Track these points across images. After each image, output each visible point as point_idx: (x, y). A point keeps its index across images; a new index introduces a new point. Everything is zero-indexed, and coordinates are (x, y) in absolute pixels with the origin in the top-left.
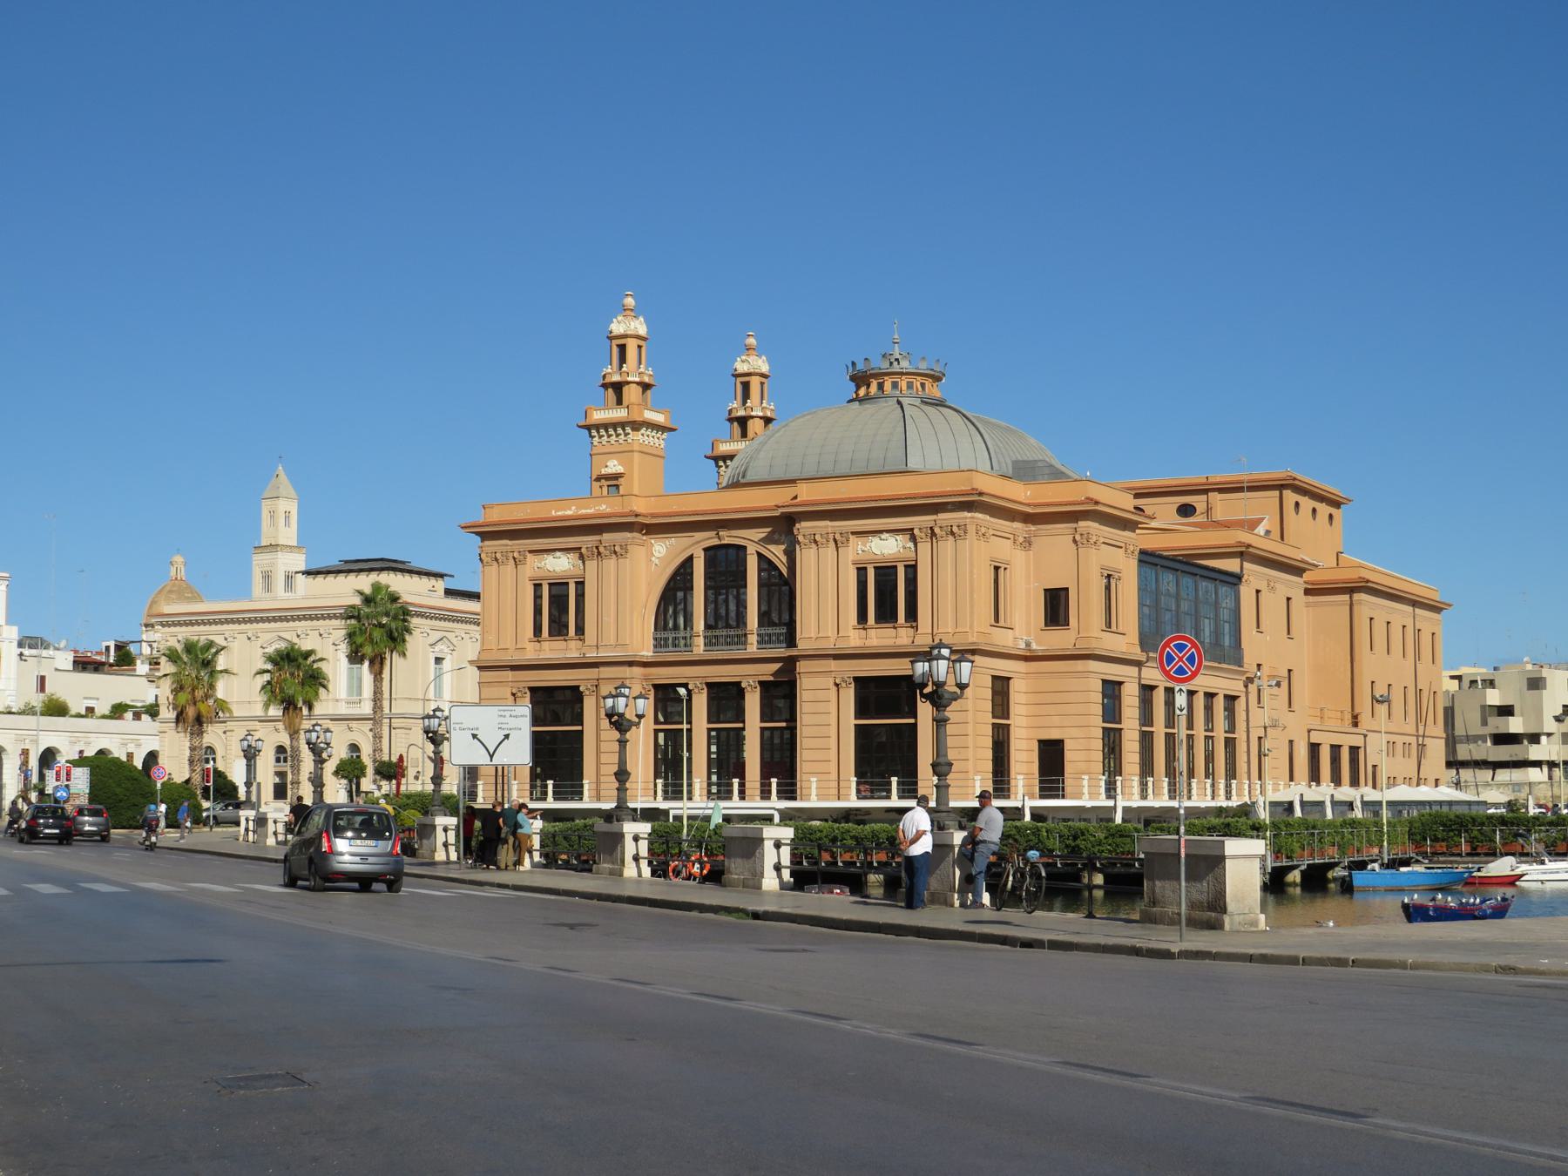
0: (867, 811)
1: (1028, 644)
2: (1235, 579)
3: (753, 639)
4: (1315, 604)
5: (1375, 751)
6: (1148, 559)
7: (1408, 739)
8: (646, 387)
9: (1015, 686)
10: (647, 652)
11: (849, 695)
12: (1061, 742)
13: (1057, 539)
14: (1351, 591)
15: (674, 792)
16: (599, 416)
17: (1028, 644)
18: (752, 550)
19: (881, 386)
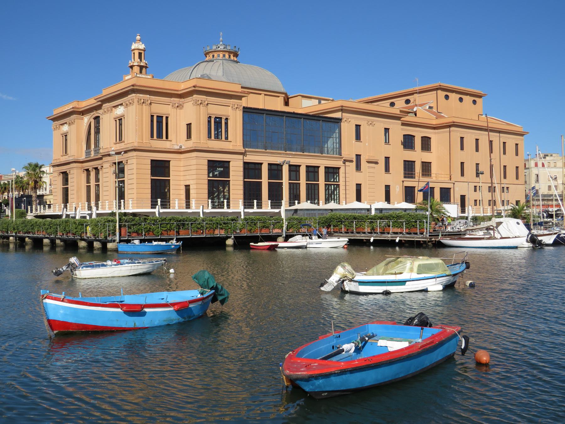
1: (181, 147)
2: (338, 121)
4: (438, 133)
6: (247, 110)
8: (141, 67)
10: (83, 157)
13: (189, 104)
14: (450, 126)
17: (181, 147)
19: (213, 56)
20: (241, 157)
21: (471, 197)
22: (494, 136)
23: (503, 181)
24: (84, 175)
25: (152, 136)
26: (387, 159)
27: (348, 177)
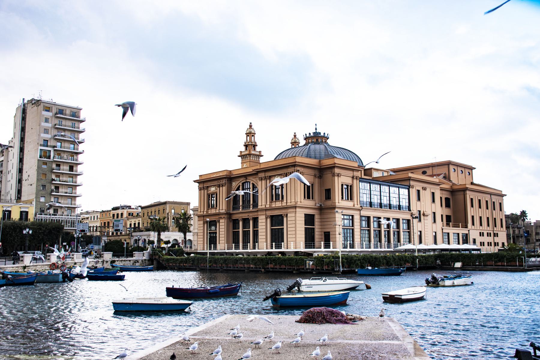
0: (271, 252)
3: (251, 206)
5: (474, 234)
7: (489, 232)
9: (317, 217)
11: (269, 220)
12: (329, 232)
15: (237, 247)
16: (243, 154)
18: (251, 183)
20: (358, 212)
21: (479, 239)
22: (487, 197)
23: (495, 229)
24: (231, 224)
25: (305, 198)
26: (434, 213)
27: (417, 226)
